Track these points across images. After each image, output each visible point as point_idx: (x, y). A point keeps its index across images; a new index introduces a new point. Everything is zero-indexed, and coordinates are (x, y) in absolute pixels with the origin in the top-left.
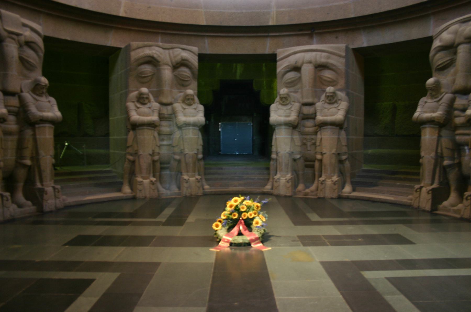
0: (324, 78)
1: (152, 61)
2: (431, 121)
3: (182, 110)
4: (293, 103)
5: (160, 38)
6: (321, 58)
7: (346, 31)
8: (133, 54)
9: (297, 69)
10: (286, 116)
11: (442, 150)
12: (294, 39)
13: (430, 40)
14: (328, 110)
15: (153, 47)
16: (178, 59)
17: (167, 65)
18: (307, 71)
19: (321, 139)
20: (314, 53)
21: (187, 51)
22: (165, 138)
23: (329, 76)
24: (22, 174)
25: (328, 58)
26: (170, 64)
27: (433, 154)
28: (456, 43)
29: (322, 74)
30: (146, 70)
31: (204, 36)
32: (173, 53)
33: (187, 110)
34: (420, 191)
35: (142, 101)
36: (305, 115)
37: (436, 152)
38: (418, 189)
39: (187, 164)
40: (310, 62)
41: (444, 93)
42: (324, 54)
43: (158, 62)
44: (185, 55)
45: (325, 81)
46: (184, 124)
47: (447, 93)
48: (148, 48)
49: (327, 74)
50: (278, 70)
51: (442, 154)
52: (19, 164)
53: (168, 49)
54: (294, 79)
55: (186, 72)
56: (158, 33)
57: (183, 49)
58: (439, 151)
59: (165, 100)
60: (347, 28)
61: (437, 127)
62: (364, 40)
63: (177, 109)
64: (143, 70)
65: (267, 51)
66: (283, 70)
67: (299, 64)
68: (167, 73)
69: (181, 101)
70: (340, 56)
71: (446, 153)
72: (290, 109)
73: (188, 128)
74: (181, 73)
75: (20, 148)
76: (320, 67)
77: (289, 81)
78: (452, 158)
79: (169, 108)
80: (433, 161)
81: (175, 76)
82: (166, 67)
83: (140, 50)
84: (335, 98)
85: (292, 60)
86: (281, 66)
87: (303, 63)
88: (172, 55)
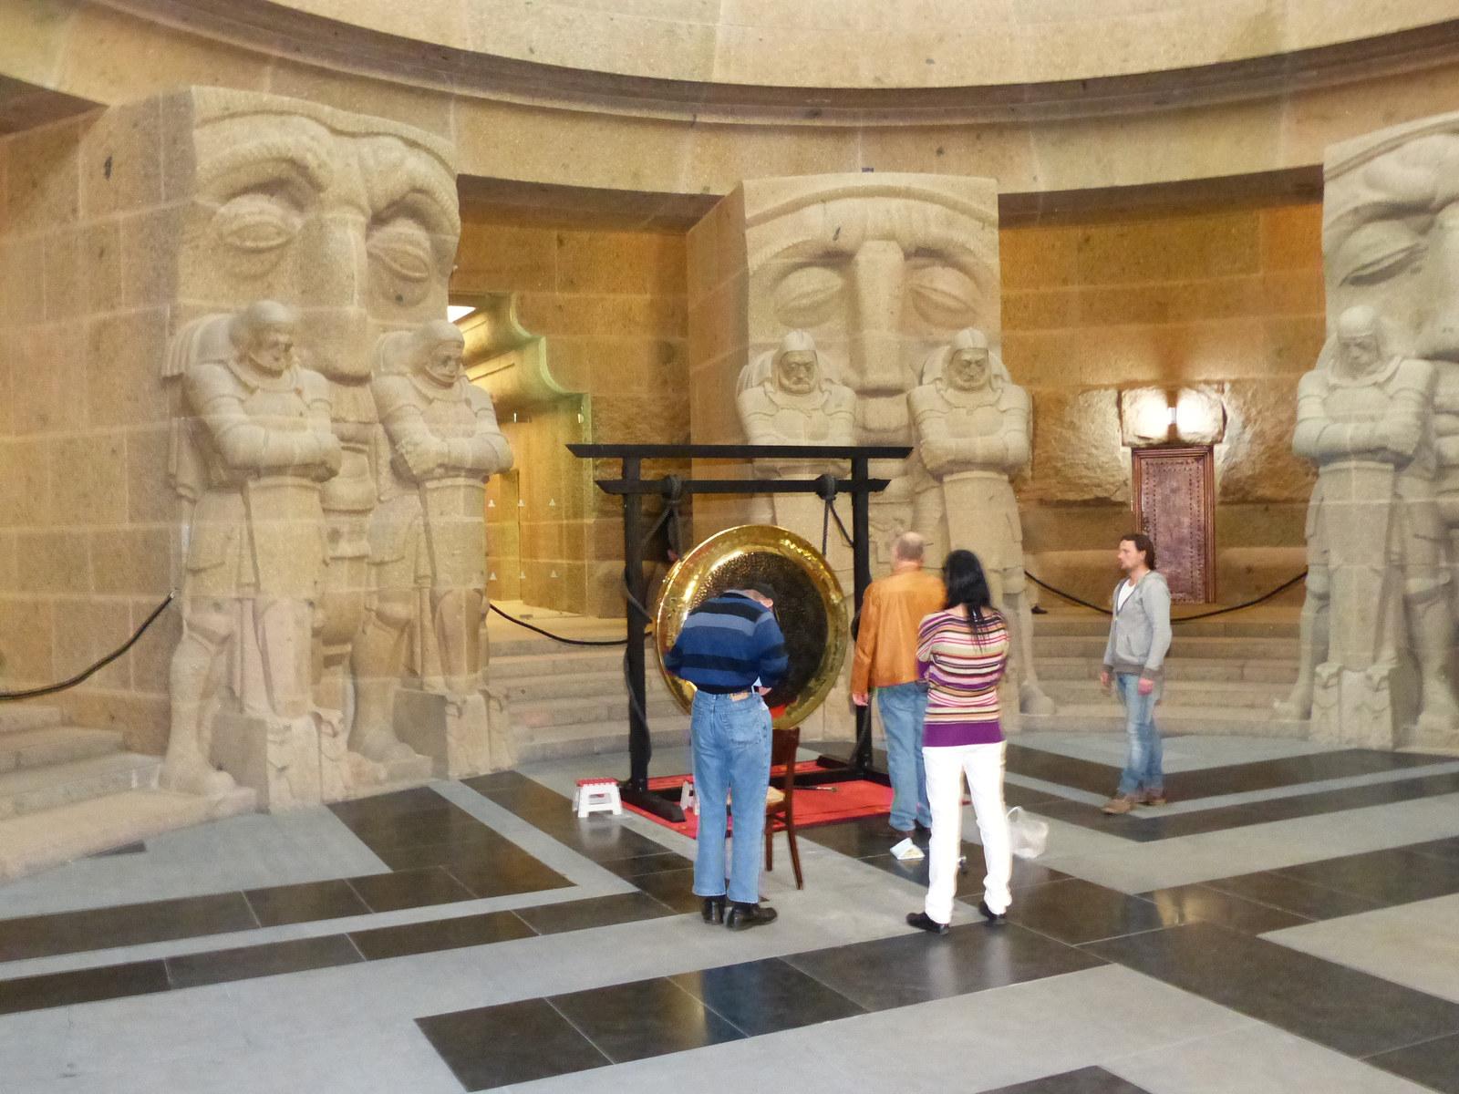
0: (934, 297)
1: (289, 182)
2: (1372, 452)
3: (422, 406)
4: (825, 386)
5: (267, 81)
6: (930, 224)
7: (978, 131)
9: (836, 258)
11: (1403, 541)
12: (784, 146)
13: (1305, 186)
14: (970, 413)
15: (295, 119)
16: (394, 184)
17: (349, 202)
18: (880, 269)
19: (944, 519)
20: (895, 203)
22: (345, 529)
23: (956, 292)
25: (950, 223)
26: (364, 202)
27: (1377, 561)
28: (1439, 199)
29: (926, 282)
31: (445, 97)
33: (436, 404)
34: (1339, 683)
35: (266, 359)
36: (870, 431)
37: (1388, 552)
38: (1331, 676)
39: (444, 638)
40: (889, 237)
41: (1397, 359)
42: (934, 210)
43: (317, 187)
44: (418, 167)
45: (937, 306)
46: (440, 466)
47: (1405, 358)
48: (276, 120)
49: (944, 282)
50: (754, 262)
51: (1402, 556)
53: (353, 135)
54: (821, 296)
56: (262, 59)
57: (412, 144)
58: (1396, 548)
59: (348, 364)
60: (982, 120)
61: (1390, 467)
62: (1044, 169)
63: (400, 402)
65: (685, 182)
66: (779, 262)
67: (845, 243)
68: (349, 240)
69: (406, 369)
70: (982, 219)
71: (1419, 551)
73: (448, 482)
76: (924, 254)
77: (805, 302)
78: (1436, 572)
79: (363, 393)
80: (1377, 584)
81: (370, 255)
84: (987, 371)
85: (817, 224)
86: (766, 246)
87: (864, 238)
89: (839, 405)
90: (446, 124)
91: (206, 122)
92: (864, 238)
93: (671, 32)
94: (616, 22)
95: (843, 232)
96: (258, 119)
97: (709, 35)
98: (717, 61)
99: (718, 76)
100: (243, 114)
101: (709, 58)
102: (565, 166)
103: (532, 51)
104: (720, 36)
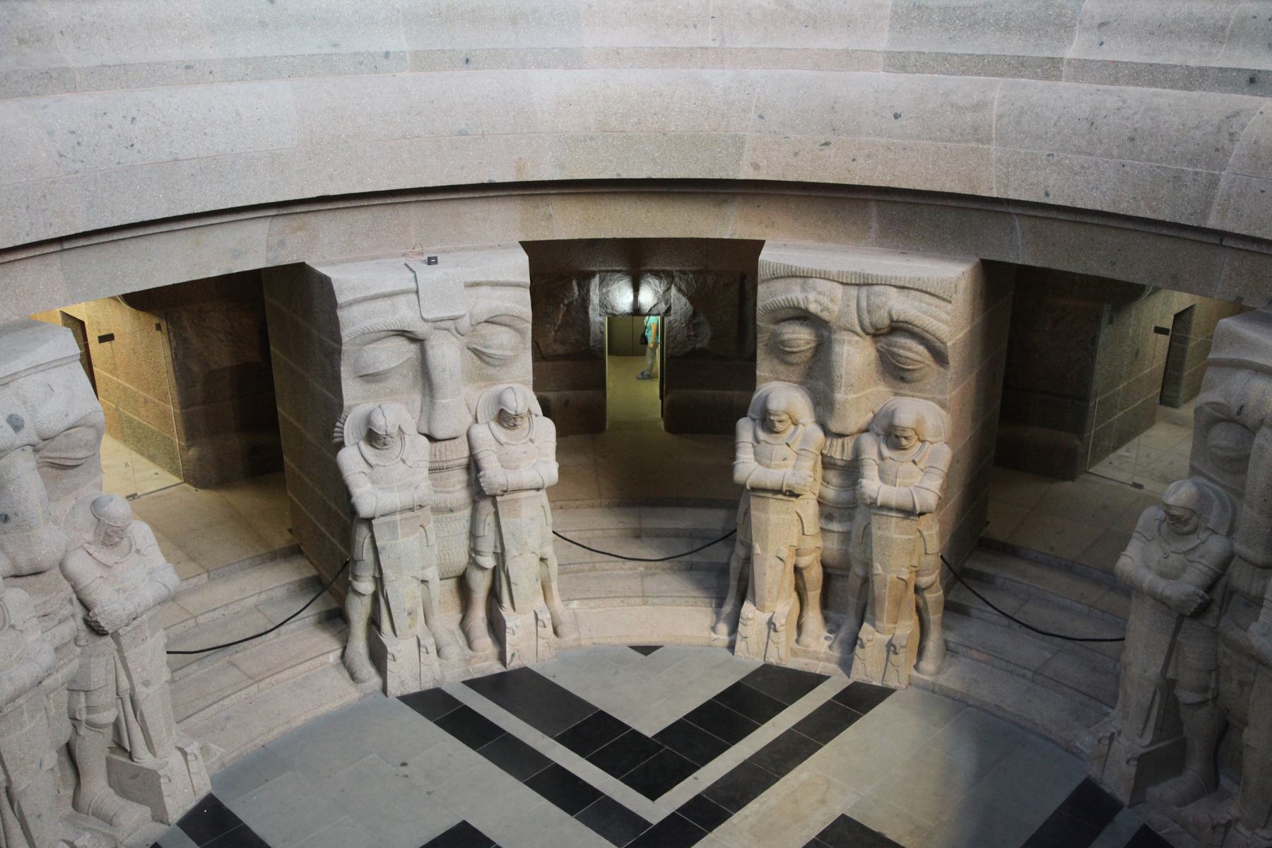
8: (761, 289)
10: (1162, 575)
15: (811, 281)
21: (913, 293)
24: (480, 584)
30: (795, 336)
32: (868, 298)
48: (800, 281)
52: (474, 563)
55: (910, 350)
56: (868, 200)
59: (835, 426)
64: (786, 337)
72: (1186, 553)
74: (895, 350)
75: (473, 535)
79: (849, 443)
82: (846, 336)
83: (778, 285)
88: (864, 304)
89: (1202, 557)
90: (1013, 228)
91: (764, 281)
92: (1262, 422)
93: (1177, 177)
94: (1127, 168)
95: (1245, 411)
96: (789, 280)
97: (1213, 182)
98: (1215, 207)
99: (1212, 222)
100: (782, 277)
101: (1209, 204)
102: (1113, 264)
103: (1047, 194)
104: (1223, 184)
